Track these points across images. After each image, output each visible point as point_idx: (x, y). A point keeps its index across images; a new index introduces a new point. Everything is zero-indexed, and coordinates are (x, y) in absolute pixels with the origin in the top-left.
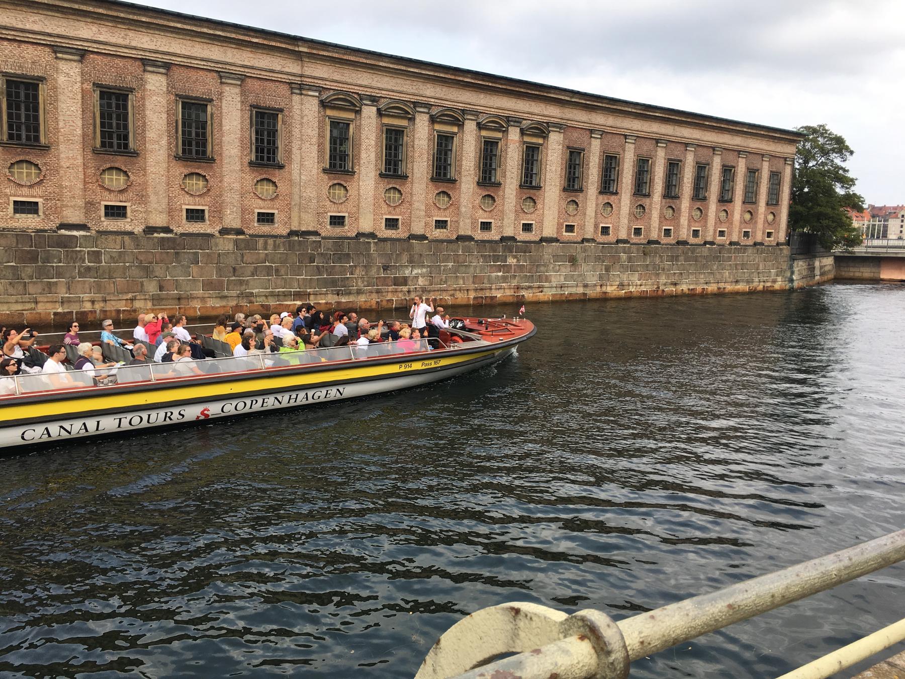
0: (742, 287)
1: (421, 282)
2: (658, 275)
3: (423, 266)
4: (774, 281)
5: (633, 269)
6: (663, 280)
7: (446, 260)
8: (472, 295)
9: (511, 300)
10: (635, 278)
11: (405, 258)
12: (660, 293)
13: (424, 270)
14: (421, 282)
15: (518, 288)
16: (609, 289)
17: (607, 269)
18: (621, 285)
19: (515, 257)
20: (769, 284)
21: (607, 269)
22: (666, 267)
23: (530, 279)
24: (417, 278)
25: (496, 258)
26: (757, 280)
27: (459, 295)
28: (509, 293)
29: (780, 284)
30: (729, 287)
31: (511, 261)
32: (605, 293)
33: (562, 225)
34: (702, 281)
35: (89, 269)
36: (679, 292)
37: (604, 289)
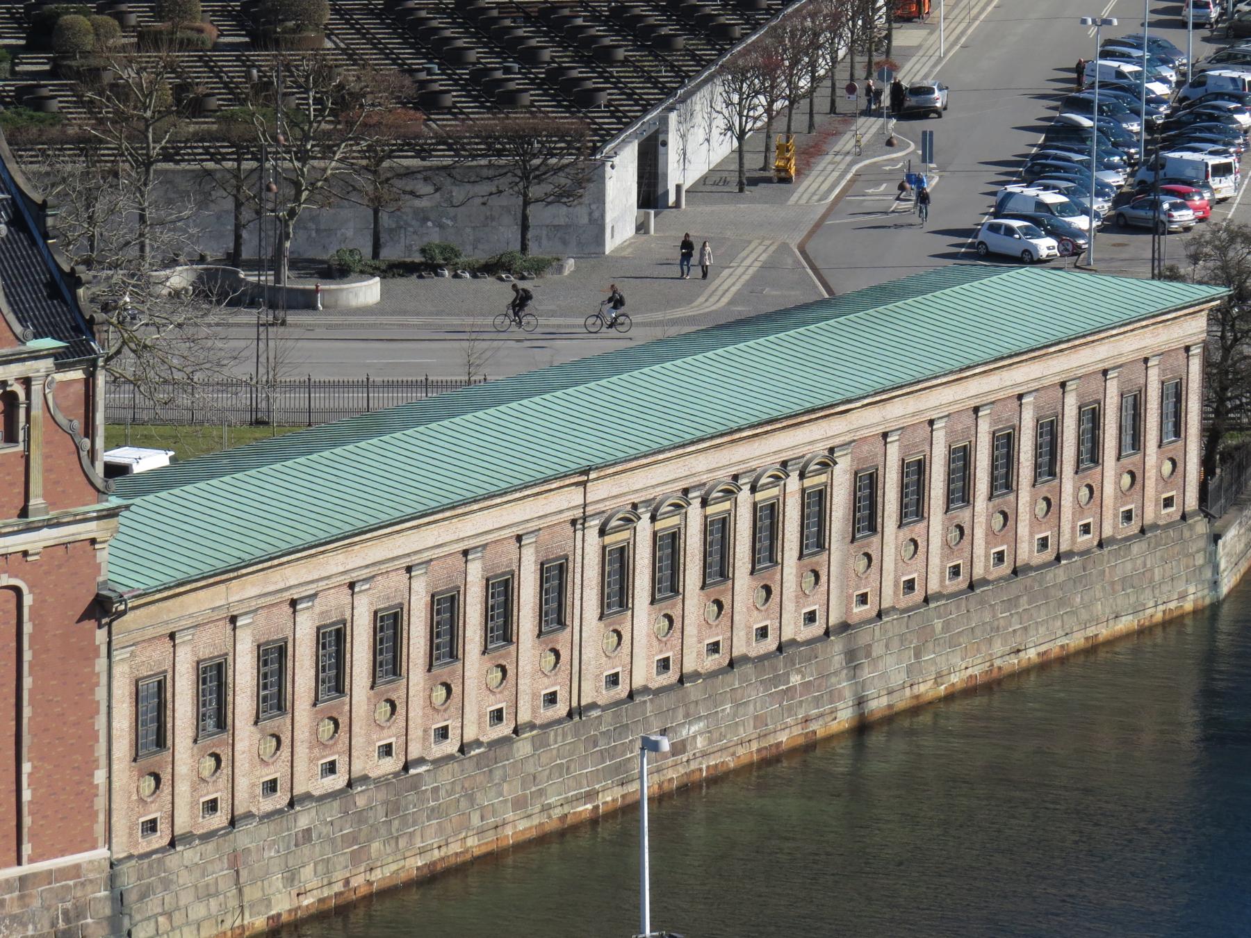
0: (1126, 623)
1: (700, 743)
2: (990, 641)
3: (700, 718)
4: (1182, 597)
5: (953, 644)
6: (998, 648)
7: (722, 703)
8: (755, 746)
9: (801, 741)
10: (956, 660)
11: (681, 713)
12: (995, 674)
13: (702, 724)
14: (700, 743)
15: (806, 720)
16: (922, 688)
17: (917, 655)
18: (938, 678)
19: (799, 671)
20: (1172, 605)
21: (917, 655)
22: (1002, 622)
23: (817, 701)
24: (695, 737)
25: (776, 681)
26: (1151, 604)
27: (741, 751)
28: (797, 731)
29: (1193, 597)
30: (1104, 632)
31: (795, 679)
32: (917, 697)
33: (851, 596)
34: (1060, 633)
35: (433, 809)
36: (1024, 664)
37: (916, 690)
